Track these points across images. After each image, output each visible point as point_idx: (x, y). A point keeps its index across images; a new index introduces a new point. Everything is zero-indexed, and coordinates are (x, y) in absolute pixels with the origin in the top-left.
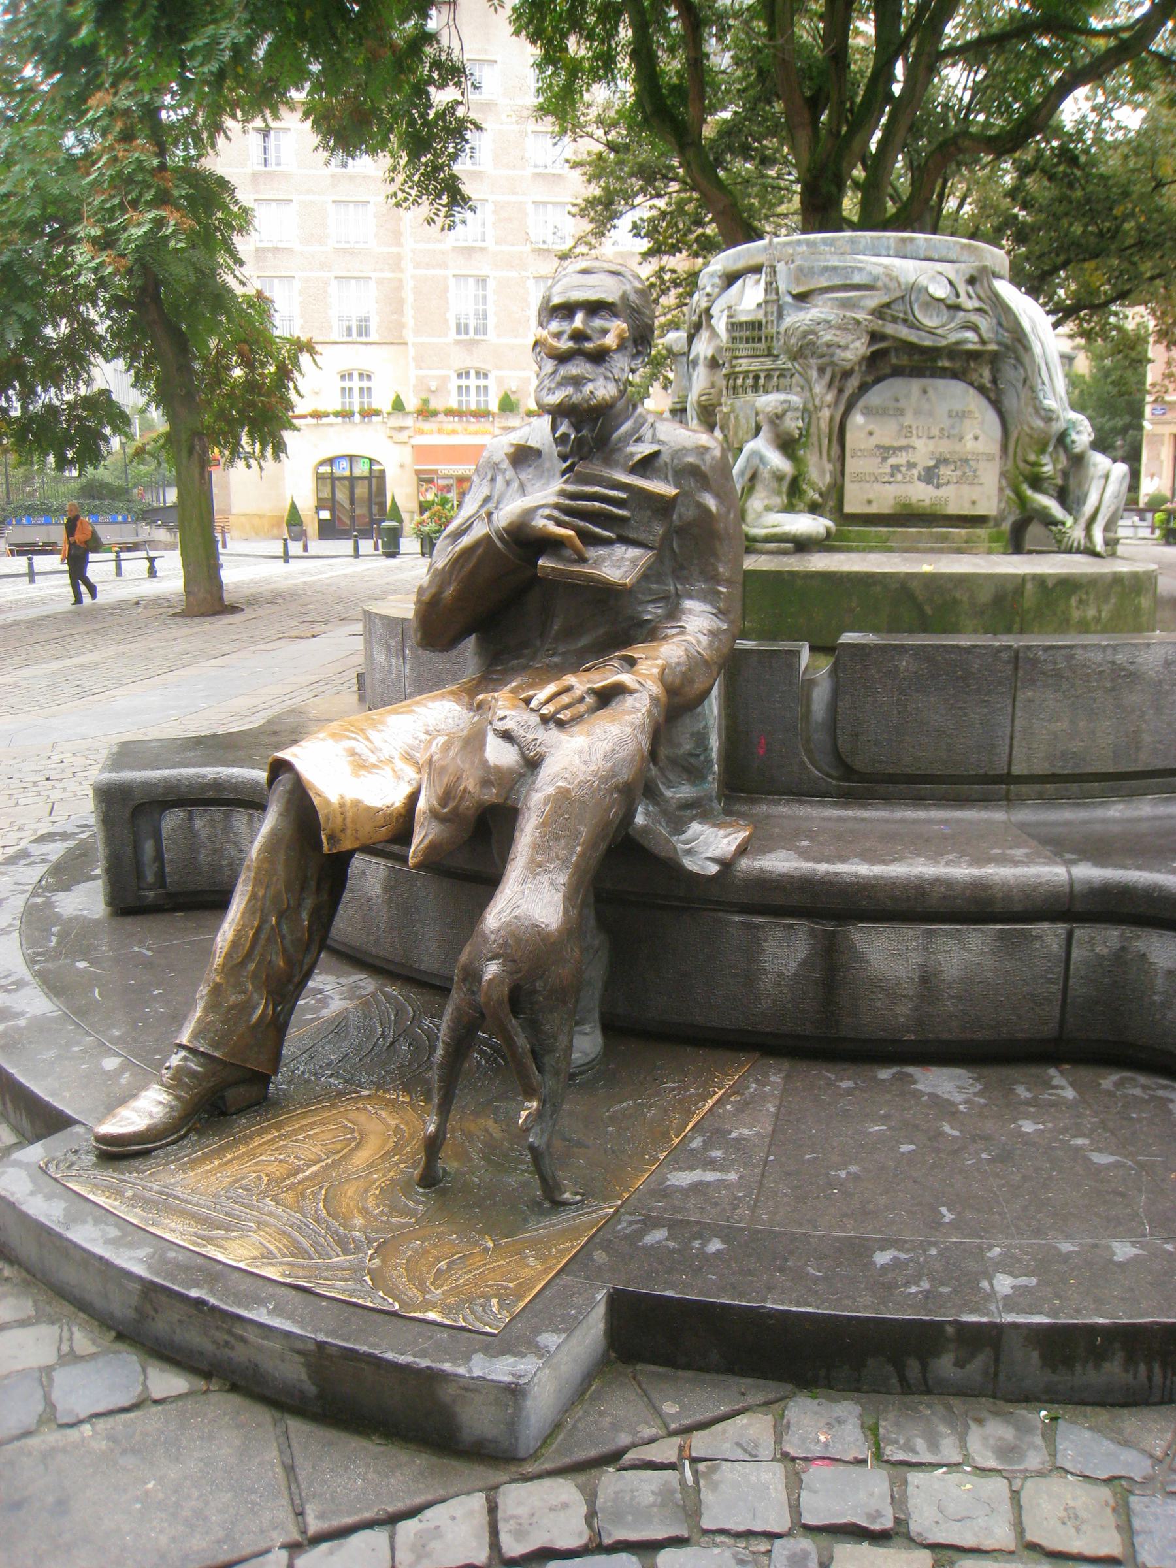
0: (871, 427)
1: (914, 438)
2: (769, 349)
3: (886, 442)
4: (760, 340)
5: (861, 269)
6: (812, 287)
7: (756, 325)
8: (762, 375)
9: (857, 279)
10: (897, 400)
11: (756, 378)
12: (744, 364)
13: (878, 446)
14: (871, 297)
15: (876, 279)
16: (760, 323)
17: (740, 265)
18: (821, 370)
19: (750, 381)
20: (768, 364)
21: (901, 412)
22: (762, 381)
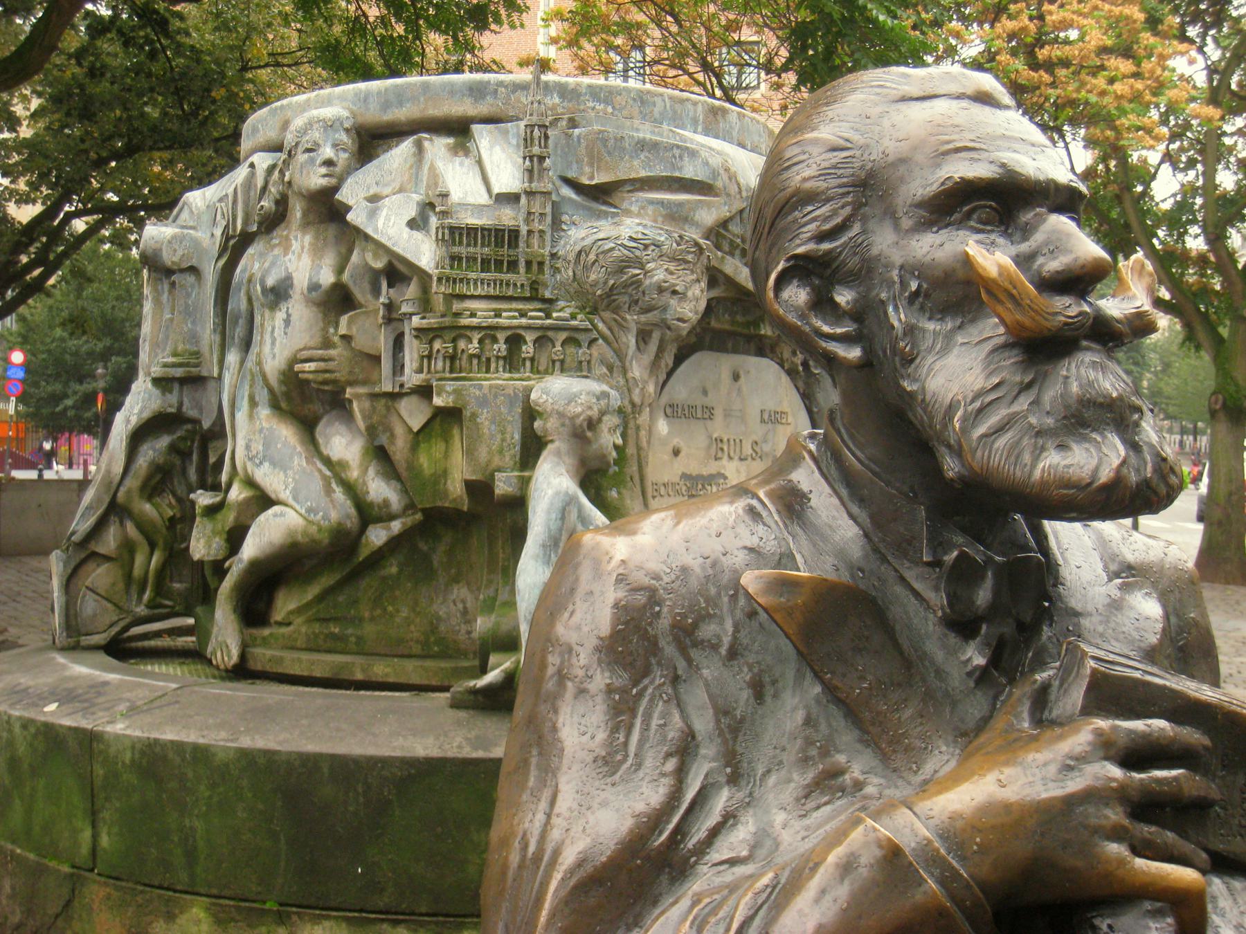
0: (676, 441)
1: (725, 461)
2: (534, 285)
3: (694, 468)
4: (513, 266)
5: (693, 154)
6: (622, 176)
7: (505, 237)
8: (530, 337)
9: (689, 171)
10: (705, 393)
11: (515, 341)
12: (480, 312)
13: (685, 476)
14: (709, 205)
15: (715, 174)
16: (514, 234)
17: (402, 113)
18: (643, 336)
19: (501, 347)
20: (535, 317)
21: (709, 413)
22: (528, 349)
